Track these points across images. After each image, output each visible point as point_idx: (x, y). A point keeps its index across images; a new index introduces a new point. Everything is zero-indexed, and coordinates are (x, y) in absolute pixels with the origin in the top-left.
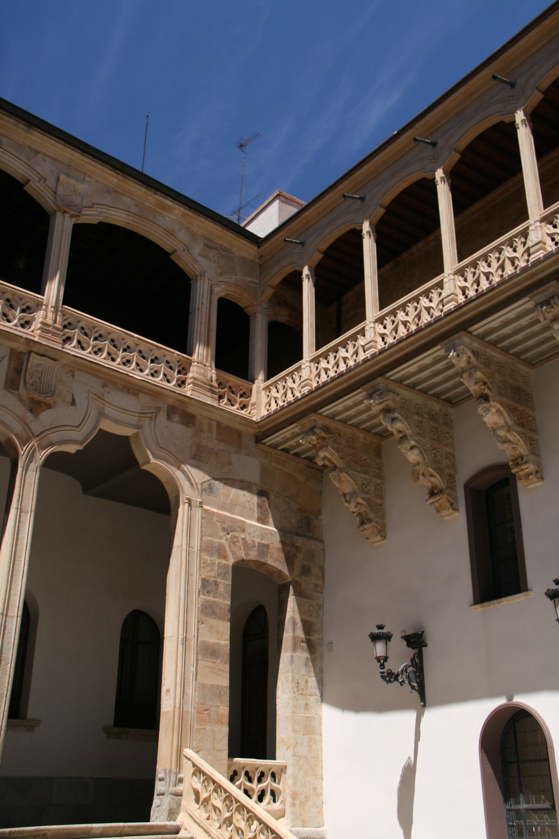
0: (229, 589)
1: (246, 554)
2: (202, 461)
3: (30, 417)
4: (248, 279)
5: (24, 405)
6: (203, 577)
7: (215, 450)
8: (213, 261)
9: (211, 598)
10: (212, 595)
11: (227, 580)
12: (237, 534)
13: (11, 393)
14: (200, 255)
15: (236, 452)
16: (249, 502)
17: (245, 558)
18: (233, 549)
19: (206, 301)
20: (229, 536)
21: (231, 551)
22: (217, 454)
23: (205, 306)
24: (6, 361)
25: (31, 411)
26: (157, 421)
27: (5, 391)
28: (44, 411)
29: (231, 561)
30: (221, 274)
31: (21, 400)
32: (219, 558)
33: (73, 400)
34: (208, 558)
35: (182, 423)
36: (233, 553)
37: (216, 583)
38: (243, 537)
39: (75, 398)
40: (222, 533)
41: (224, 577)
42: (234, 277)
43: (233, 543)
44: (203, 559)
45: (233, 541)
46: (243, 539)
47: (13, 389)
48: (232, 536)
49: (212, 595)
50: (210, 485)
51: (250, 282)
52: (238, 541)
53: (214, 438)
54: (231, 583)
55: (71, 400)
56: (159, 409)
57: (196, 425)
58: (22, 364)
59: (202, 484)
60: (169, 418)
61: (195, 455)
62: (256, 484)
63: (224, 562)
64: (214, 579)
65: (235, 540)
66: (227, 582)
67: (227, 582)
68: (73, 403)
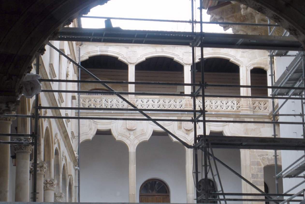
0: (263, 176)
1: (269, 163)
3: (186, 136)
4: (263, 58)
6: (252, 173)
8: (246, 57)
9: (256, 180)
10: (256, 179)
11: (261, 173)
12: (264, 157)
13: (180, 130)
14: (240, 57)
15: (263, 127)
17: (268, 164)
18: (263, 162)
19: (245, 75)
20: (261, 158)
21: (263, 163)
22: (254, 130)
25: (187, 134)
26: (229, 125)
27: (178, 130)
28: (191, 133)
29: (263, 166)
30: (250, 61)
31: (183, 132)
32: (258, 166)
33: (199, 127)
34: (253, 167)
36: (263, 163)
37: (257, 174)
38: (267, 157)
39: (200, 126)
40: (258, 157)
41: (260, 172)
42: (256, 60)
43: (263, 160)
44: (251, 167)
45: (263, 159)
46: (267, 158)
48: (262, 157)
49: (256, 179)
52: (265, 159)
54: (263, 173)
55: (199, 127)
63: (260, 167)
64: (256, 173)
66: (262, 173)
67: (262, 173)
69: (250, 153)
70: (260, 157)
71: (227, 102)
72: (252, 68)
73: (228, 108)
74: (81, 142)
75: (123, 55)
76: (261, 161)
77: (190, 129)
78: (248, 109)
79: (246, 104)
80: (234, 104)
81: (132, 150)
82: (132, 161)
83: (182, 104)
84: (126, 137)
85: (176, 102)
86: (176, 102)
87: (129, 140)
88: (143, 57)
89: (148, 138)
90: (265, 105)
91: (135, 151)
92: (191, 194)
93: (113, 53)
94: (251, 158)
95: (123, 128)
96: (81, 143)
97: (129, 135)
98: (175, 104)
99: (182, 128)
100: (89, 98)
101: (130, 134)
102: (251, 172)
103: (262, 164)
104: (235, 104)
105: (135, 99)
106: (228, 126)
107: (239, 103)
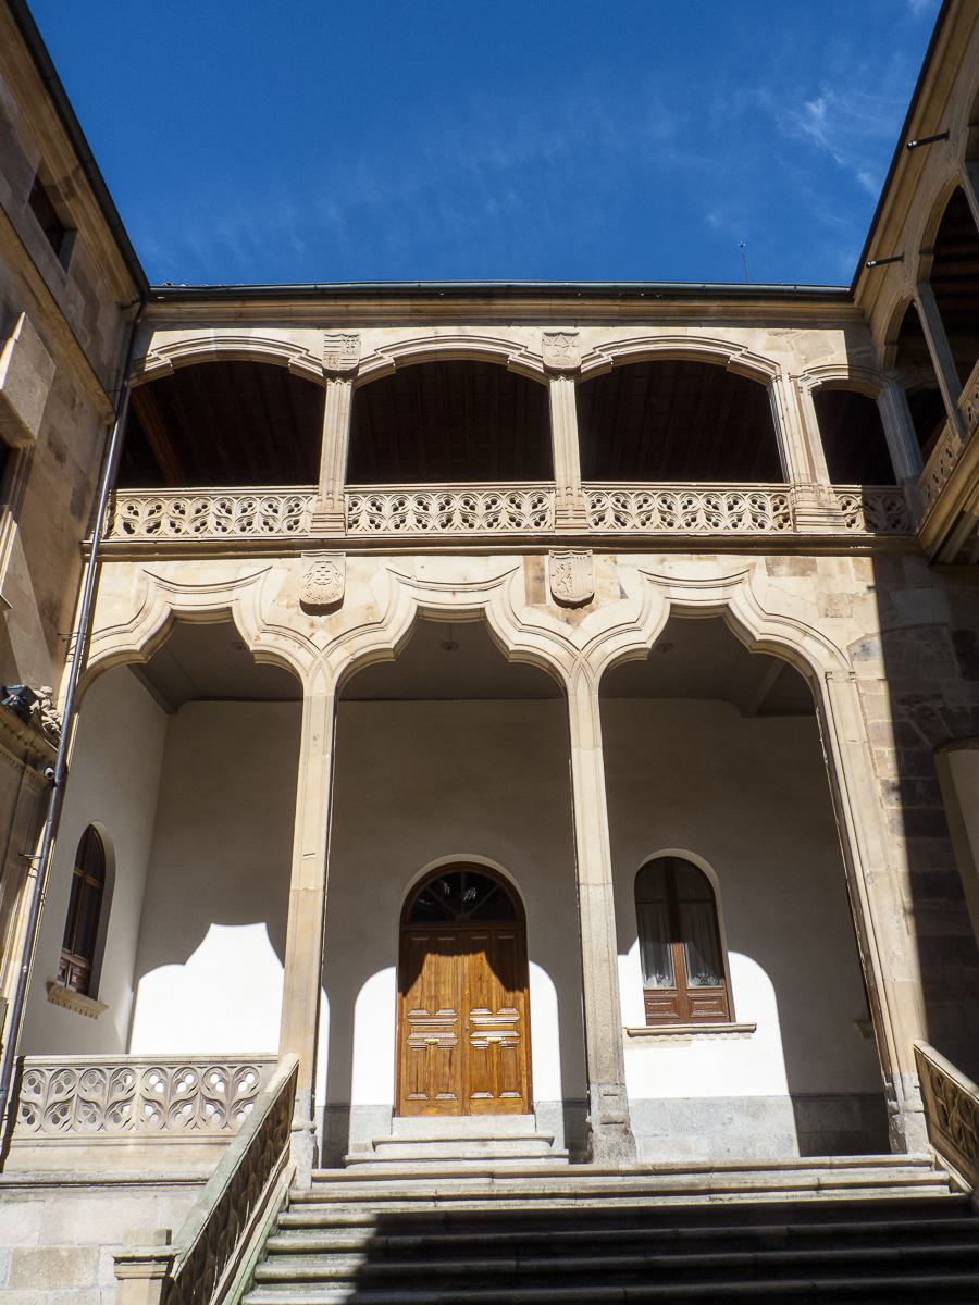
2: (842, 617)
3: (566, 630)
5: (557, 617)
7: (861, 595)
12: (928, 705)
13: (537, 608)
14: (767, 349)
16: (940, 652)
23: (791, 411)
24: (521, 571)
25: (567, 621)
27: (527, 608)
28: (585, 616)
31: (552, 613)
33: (622, 592)
35: (795, 574)
39: (624, 587)
46: (943, 709)
47: (538, 602)
50: (863, 646)
51: (859, 353)
53: (854, 579)
55: (619, 593)
56: (754, 565)
57: (818, 570)
58: (543, 570)
59: (848, 647)
60: (771, 572)
61: (827, 610)
62: (947, 625)
65: (927, 713)
68: (623, 595)
69: (861, 691)
70: (906, 707)
71: (731, 500)
72: (817, 380)
73: (740, 524)
74: (90, 663)
75: (304, 352)
76: (912, 722)
77: (580, 600)
78: (824, 519)
79: (815, 505)
80: (762, 508)
81: (319, 693)
82: (315, 738)
83: (545, 511)
84: (296, 640)
85: (518, 507)
86: (518, 507)
87: (309, 650)
88: (386, 356)
89: (395, 641)
90: (889, 509)
91: (333, 693)
92: (597, 885)
93: (269, 345)
94: (866, 711)
95: (285, 603)
96: (93, 666)
97: (306, 631)
98: (514, 510)
99: (544, 596)
100: (156, 498)
101: (312, 625)
102: (875, 770)
103: (925, 739)
104: (769, 506)
105: (347, 496)
106: (747, 586)
107: (782, 502)
